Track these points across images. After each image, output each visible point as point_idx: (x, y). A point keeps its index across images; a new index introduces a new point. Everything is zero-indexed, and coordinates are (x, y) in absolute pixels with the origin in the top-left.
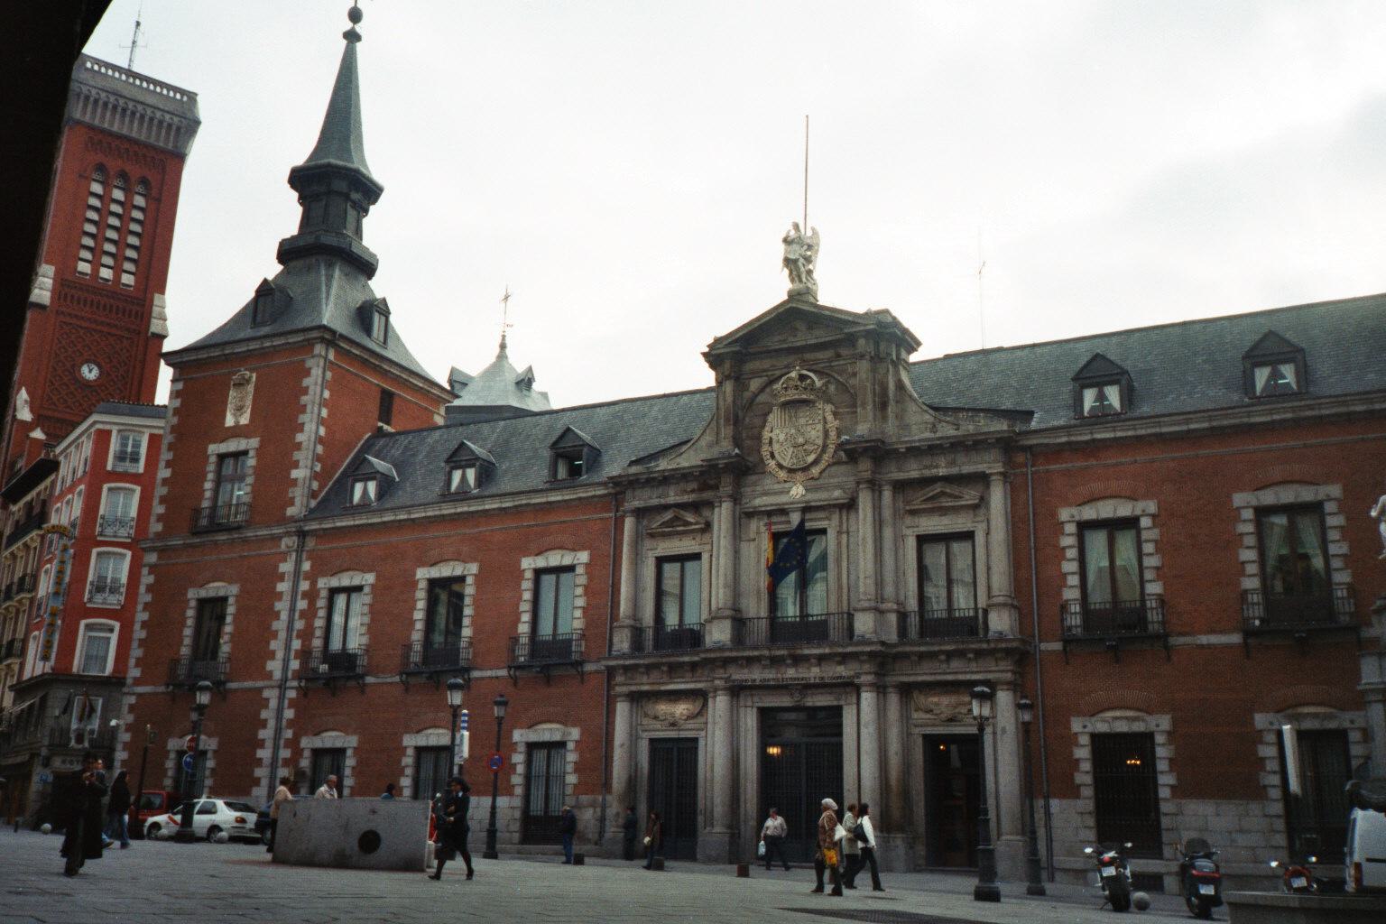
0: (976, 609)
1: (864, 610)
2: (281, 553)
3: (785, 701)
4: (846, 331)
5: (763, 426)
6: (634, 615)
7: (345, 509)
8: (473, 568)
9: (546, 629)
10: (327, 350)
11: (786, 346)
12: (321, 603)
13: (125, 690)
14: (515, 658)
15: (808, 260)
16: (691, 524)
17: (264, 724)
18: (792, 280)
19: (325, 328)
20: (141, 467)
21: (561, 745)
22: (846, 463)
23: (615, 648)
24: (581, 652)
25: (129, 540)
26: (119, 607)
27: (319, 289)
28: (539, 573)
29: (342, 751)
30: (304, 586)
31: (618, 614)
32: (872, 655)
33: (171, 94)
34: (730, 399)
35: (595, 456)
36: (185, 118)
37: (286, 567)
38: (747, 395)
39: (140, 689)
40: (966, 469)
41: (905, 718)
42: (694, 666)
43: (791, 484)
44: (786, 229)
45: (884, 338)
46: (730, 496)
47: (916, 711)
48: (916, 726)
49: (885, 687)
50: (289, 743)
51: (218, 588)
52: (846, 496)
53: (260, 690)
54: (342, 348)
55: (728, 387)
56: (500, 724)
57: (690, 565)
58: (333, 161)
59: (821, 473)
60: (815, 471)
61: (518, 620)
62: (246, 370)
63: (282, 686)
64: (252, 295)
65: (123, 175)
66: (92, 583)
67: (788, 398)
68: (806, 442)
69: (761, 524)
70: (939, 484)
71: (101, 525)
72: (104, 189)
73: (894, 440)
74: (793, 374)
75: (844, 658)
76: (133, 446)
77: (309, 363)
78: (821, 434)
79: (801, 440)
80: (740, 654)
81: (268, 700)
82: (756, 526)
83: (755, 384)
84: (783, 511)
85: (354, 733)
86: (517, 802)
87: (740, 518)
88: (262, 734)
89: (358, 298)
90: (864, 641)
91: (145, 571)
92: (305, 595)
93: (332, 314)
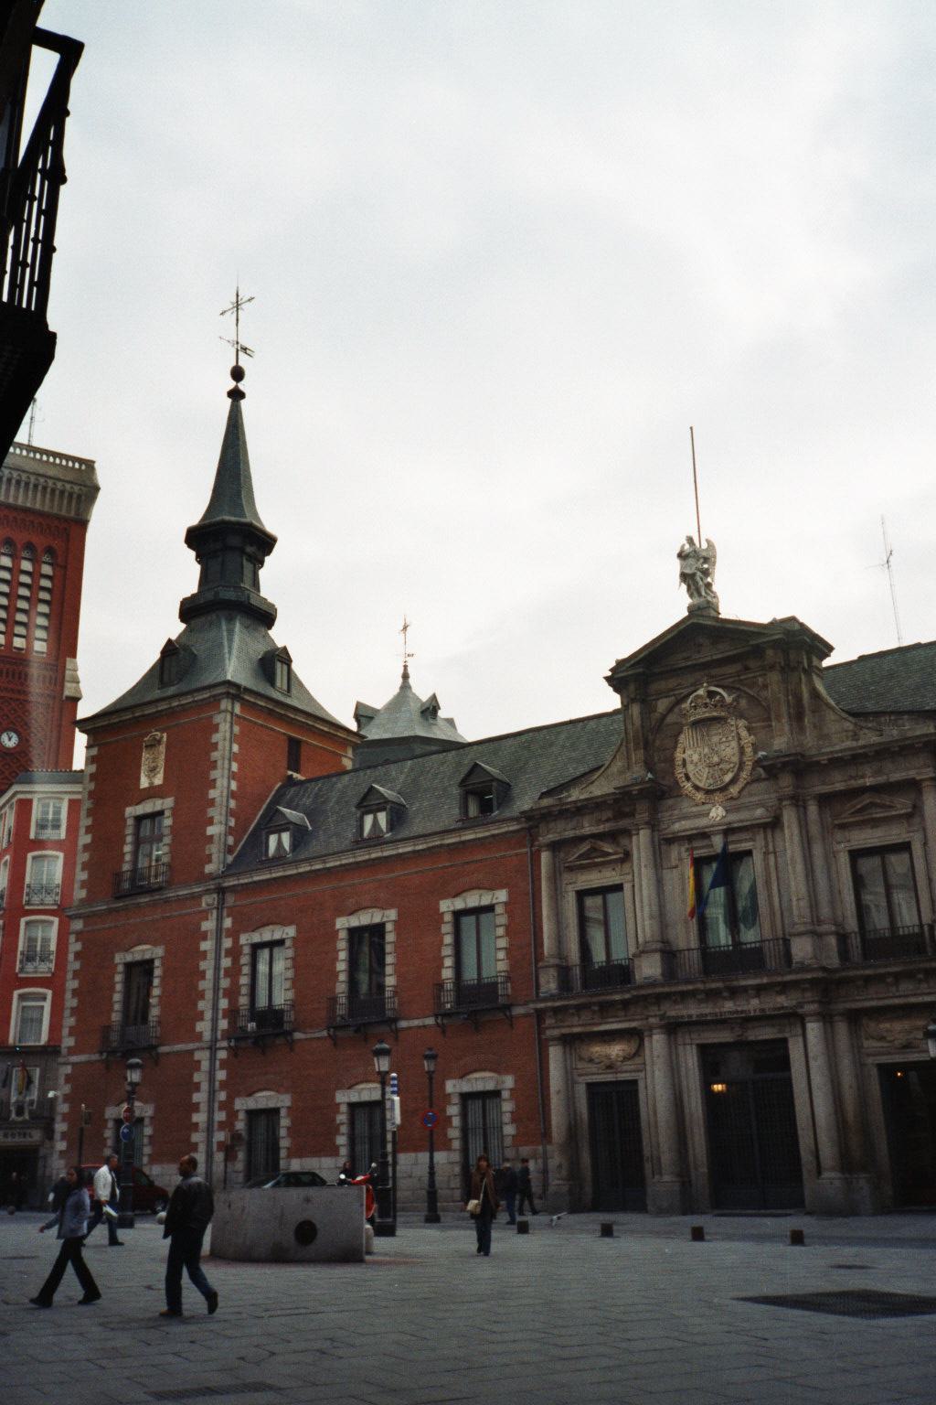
0: (921, 926)
1: (800, 934)
2: (200, 912)
3: (724, 1036)
4: (751, 643)
5: (675, 748)
6: (559, 954)
7: (262, 862)
8: (392, 914)
9: (470, 974)
10: (233, 704)
11: (690, 663)
12: (245, 960)
13: (61, 1060)
14: (440, 1005)
15: (706, 573)
16: (609, 854)
17: (197, 1087)
18: (691, 596)
19: (229, 683)
20: (63, 834)
21: (496, 1094)
22: (764, 780)
23: (543, 989)
24: (508, 995)
25: (55, 907)
26: (49, 975)
27: (221, 645)
28: (458, 915)
29: (276, 1111)
30: (227, 943)
31: (542, 953)
32: (814, 983)
33: (70, 464)
34: (637, 722)
35: (505, 791)
36: (85, 486)
37: (208, 925)
38: (656, 715)
39: (74, 1059)
40: (897, 776)
41: (857, 1049)
42: (625, 1004)
43: (710, 806)
44: (679, 543)
45: (793, 645)
46: (647, 823)
47: (867, 1039)
48: (868, 1055)
49: (831, 1016)
50: (223, 1106)
51: (143, 951)
52: (768, 814)
53: (191, 1052)
54: (248, 701)
55: (635, 710)
56: (431, 1079)
57: (612, 897)
58: (227, 518)
59: (739, 792)
60: (734, 790)
61: (441, 966)
62: (157, 731)
63: (213, 1049)
64: (157, 656)
65: (30, 546)
66: (22, 953)
67: (698, 717)
68: (722, 761)
69: (683, 849)
70: (867, 795)
71: (28, 894)
72: (13, 562)
73: (814, 752)
74: (701, 692)
75: (784, 988)
76: (54, 813)
77: (218, 719)
78: (736, 750)
79: (716, 759)
80: (674, 989)
81: (199, 1062)
82: (678, 853)
83: (662, 705)
84: (704, 835)
85: (287, 1092)
86: (456, 1157)
87: (660, 845)
88: (196, 1097)
89: (259, 649)
90: (804, 968)
91: (72, 938)
92: (229, 953)
93: (235, 669)
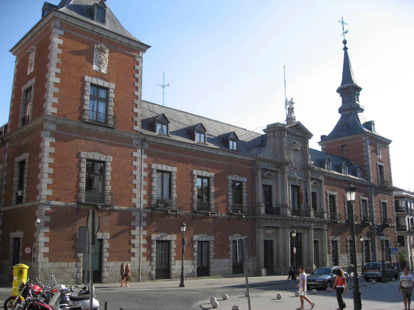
86: (231, 261)
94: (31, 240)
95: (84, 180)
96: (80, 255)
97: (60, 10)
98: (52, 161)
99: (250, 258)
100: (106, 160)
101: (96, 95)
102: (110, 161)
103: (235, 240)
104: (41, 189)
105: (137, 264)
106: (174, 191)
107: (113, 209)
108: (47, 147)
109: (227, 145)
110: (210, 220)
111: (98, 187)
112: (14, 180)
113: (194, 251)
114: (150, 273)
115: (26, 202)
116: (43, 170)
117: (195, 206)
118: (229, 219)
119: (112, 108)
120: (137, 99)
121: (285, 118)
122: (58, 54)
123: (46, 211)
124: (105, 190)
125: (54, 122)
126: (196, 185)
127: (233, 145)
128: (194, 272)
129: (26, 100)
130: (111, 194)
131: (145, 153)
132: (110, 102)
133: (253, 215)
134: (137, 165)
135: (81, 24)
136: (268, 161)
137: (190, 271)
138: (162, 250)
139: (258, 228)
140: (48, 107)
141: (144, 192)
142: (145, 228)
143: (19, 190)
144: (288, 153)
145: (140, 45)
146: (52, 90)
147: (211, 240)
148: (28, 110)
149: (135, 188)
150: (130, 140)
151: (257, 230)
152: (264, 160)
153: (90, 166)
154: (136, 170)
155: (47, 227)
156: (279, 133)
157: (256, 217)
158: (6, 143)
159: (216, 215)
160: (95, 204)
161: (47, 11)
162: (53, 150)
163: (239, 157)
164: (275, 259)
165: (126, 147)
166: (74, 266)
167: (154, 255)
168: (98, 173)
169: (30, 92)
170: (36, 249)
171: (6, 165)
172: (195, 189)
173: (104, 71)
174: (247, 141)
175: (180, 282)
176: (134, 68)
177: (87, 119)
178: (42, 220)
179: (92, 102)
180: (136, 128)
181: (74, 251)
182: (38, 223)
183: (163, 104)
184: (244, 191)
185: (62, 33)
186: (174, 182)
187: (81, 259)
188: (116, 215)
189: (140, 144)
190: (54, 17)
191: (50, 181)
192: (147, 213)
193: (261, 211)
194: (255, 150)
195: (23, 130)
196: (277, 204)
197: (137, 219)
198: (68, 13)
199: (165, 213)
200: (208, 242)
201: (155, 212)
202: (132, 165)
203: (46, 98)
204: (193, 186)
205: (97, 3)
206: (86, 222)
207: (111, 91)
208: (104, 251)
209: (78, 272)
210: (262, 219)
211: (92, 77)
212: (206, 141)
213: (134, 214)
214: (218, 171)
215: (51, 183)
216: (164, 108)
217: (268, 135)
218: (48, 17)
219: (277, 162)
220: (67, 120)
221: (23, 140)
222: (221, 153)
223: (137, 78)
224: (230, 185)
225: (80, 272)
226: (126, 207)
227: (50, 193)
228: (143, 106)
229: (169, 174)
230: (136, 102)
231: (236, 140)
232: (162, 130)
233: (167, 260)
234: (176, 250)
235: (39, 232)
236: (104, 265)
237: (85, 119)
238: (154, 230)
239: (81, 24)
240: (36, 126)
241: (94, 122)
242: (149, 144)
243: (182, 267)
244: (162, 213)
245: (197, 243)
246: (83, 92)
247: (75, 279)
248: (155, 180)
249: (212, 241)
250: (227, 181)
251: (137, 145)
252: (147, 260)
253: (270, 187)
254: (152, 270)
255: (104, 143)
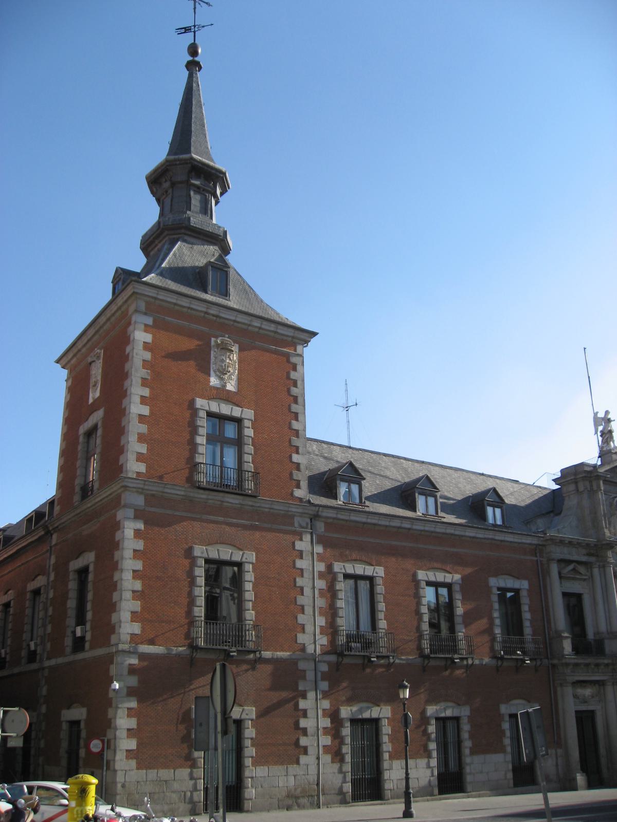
86: (509, 758)
94: (101, 725)
95: (201, 601)
96: (199, 755)
97: (144, 279)
98: (139, 565)
99: (549, 751)
100: (244, 560)
101: (218, 434)
102: (251, 561)
103: (514, 712)
104: (120, 622)
105: (313, 770)
106: (381, 616)
107: (261, 657)
108: (128, 539)
109: (483, 517)
110: (458, 672)
111: (229, 614)
112: (68, 607)
113: (429, 739)
114: (341, 788)
115: (92, 648)
116: (122, 585)
117: (426, 644)
118: (497, 668)
119: (251, 456)
120: (297, 436)
121: (596, 452)
122: (143, 360)
123: (130, 665)
124: (243, 619)
125: (140, 490)
126: (424, 601)
127: (494, 515)
128: (432, 784)
129: (87, 452)
130: (255, 626)
131: (318, 542)
132: (246, 446)
133: (547, 658)
134: (304, 567)
135: (184, 302)
136: (570, 543)
137: (424, 782)
138: (363, 739)
139: (561, 685)
140: (128, 462)
141: (321, 621)
142: (326, 695)
143: (77, 625)
144: (610, 524)
145: (296, 332)
146: (135, 428)
147: (462, 714)
148: (92, 469)
149: (303, 613)
150: (288, 518)
151: (559, 689)
152: (561, 542)
153: (212, 573)
154: (302, 576)
155: (132, 698)
156: (587, 483)
157: (555, 661)
158: (52, 535)
159: (470, 662)
160: (225, 648)
161: (120, 283)
162: (140, 545)
163: (509, 538)
164: (602, 751)
165: (280, 531)
166: (187, 777)
167: (347, 749)
168: (228, 586)
169: (94, 436)
170: (112, 742)
171: (52, 577)
172: (424, 610)
173: (231, 386)
174: (523, 504)
175: (402, 807)
176: (288, 377)
177: (202, 480)
178: (122, 683)
179: (210, 447)
180: (298, 493)
181: (185, 745)
182: (114, 690)
183: (349, 442)
184: (525, 608)
185: (149, 321)
186: (380, 598)
187: (201, 762)
188: (269, 668)
189: (307, 524)
190: (134, 293)
191: (137, 606)
192: (329, 663)
193: (563, 648)
194: (541, 523)
195: (85, 507)
196: (597, 633)
197: (310, 675)
198: (160, 284)
199: (366, 661)
200: (457, 719)
201: (346, 660)
202: (294, 567)
203: (124, 446)
204: (419, 604)
205: (212, 260)
206: (209, 687)
207: (247, 423)
208: (246, 744)
209: (195, 788)
210: (567, 665)
211: (209, 399)
212: (439, 511)
213: (302, 665)
214: (468, 570)
215: (139, 609)
216: (350, 451)
217: (565, 489)
218: (123, 294)
219: (588, 545)
220: (166, 484)
221: (84, 527)
222: (470, 533)
223: (295, 395)
224: (495, 598)
225: (198, 788)
226: (286, 652)
227: (136, 628)
228: (310, 450)
229: (368, 582)
230: (296, 441)
231: (501, 505)
232: (349, 493)
233: (375, 759)
234: (392, 739)
235: (117, 708)
236: (247, 773)
237: (199, 481)
238: (344, 698)
239: (184, 302)
240: (106, 499)
241: (218, 487)
242: (326, 523)
243: (407, 774)
244: (360, 661)
245: (433, 722)
246: (194, 430)
247: (189, 803)
248: (341, 595)
249: (467, 717)
250: (488, 589)
251: (303, 527)
252: (333, 762)
253: (579, 596)
254: (344, 781)
255: (238, 527)
